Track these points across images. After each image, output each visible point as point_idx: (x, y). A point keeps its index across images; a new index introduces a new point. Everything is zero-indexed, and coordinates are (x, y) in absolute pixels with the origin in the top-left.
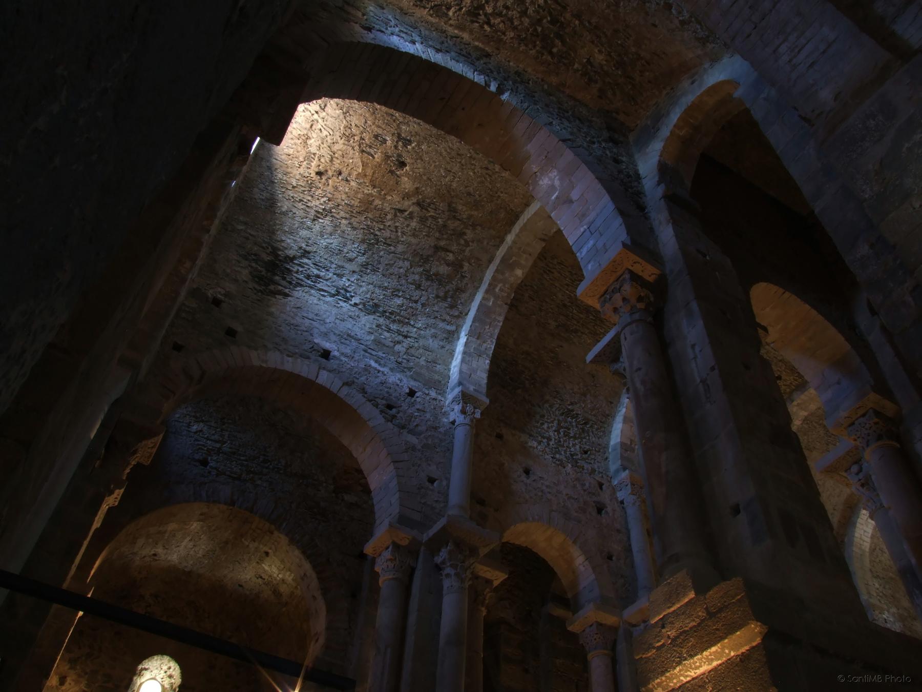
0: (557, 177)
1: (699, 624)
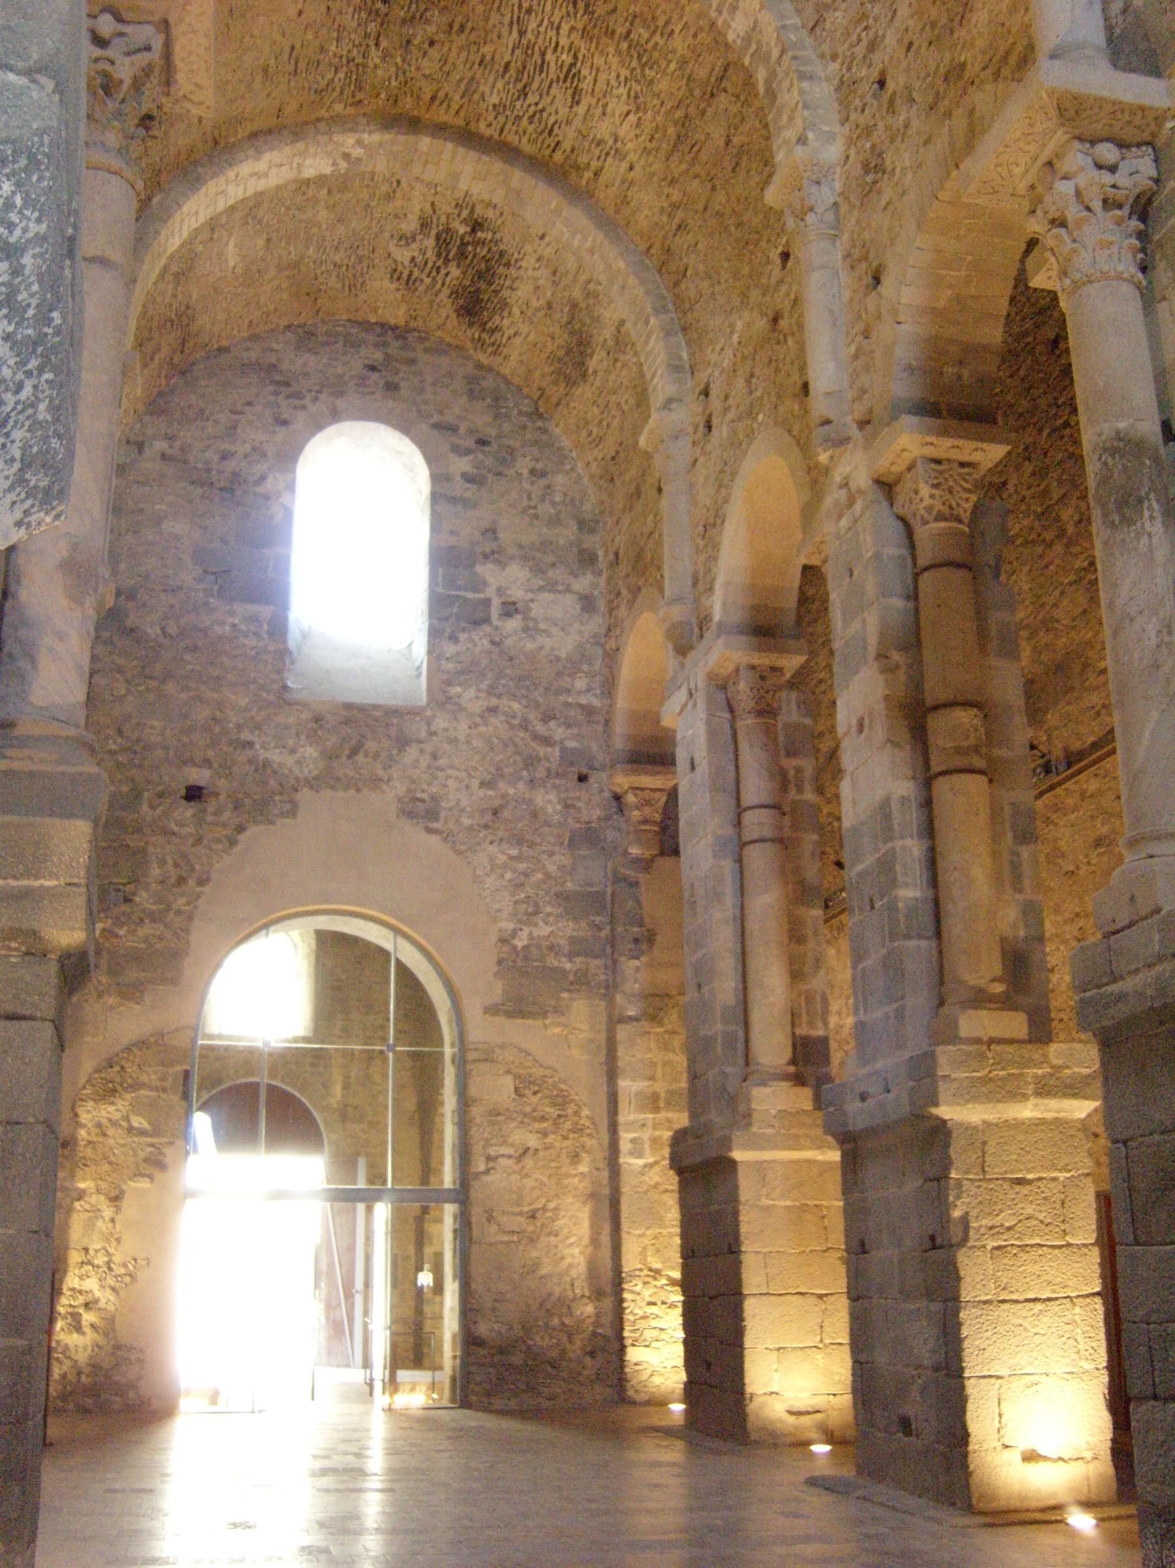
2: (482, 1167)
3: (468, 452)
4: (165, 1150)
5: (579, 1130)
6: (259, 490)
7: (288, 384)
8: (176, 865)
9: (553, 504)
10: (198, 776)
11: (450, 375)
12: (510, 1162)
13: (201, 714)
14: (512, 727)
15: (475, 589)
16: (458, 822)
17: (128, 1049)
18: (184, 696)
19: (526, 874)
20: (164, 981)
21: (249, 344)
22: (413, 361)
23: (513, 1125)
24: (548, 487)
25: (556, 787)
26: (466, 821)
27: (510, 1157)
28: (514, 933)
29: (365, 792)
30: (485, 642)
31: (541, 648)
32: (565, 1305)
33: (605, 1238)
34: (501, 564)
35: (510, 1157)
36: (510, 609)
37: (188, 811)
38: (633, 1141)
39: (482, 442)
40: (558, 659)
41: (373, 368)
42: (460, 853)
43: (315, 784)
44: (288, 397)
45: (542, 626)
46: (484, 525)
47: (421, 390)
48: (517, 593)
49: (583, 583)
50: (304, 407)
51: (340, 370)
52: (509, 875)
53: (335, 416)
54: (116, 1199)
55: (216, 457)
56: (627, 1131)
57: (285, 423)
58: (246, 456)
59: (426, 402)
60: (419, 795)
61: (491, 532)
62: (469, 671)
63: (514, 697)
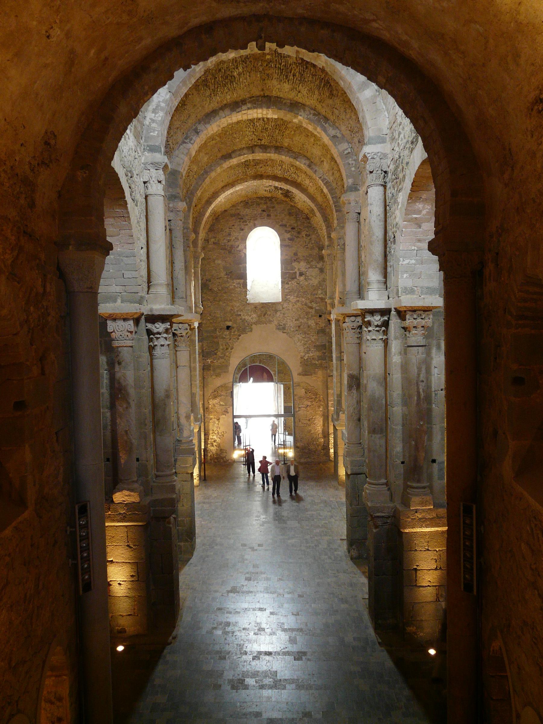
0: (428, 210)
1: (432, 518)
2: (298, 410)
3: (289, 232)
4: (228, 409)
7: (243, 219)
10: (229, 324)
11: (284, 210)
12: (304, 408)
13: (229, 309)
15: (292, 270)
17: (218, 387)
18: (224, 305)
19: (307, 341)
20: (225, 372)
21: (232, 208)
22: (274, 207)
23: (305, 400)
25: (314, 319)
26: (292, 330)
27: (304, 407)
33: (326, 425)
34: (299, 262)
35: (304, 407)
36: (301, 274)
37: (227, 332)
38: (332, 404)
39: (293, 228)
40: (314, 286)
41: (264, 211)
42: (290, 337)
43: (256, 323)
44: (243, 222)
46: (294, 252)
48: (303, 270)
49: (319, 265)
50: (247, 225)
51: (255, 212)
52: (303, 342)
53: (255, 226)
54: (218, 419)
55: (227, 241)
57: (242, 230)
59: (278, 219)
61: (296, 254)
63: (303, 297)
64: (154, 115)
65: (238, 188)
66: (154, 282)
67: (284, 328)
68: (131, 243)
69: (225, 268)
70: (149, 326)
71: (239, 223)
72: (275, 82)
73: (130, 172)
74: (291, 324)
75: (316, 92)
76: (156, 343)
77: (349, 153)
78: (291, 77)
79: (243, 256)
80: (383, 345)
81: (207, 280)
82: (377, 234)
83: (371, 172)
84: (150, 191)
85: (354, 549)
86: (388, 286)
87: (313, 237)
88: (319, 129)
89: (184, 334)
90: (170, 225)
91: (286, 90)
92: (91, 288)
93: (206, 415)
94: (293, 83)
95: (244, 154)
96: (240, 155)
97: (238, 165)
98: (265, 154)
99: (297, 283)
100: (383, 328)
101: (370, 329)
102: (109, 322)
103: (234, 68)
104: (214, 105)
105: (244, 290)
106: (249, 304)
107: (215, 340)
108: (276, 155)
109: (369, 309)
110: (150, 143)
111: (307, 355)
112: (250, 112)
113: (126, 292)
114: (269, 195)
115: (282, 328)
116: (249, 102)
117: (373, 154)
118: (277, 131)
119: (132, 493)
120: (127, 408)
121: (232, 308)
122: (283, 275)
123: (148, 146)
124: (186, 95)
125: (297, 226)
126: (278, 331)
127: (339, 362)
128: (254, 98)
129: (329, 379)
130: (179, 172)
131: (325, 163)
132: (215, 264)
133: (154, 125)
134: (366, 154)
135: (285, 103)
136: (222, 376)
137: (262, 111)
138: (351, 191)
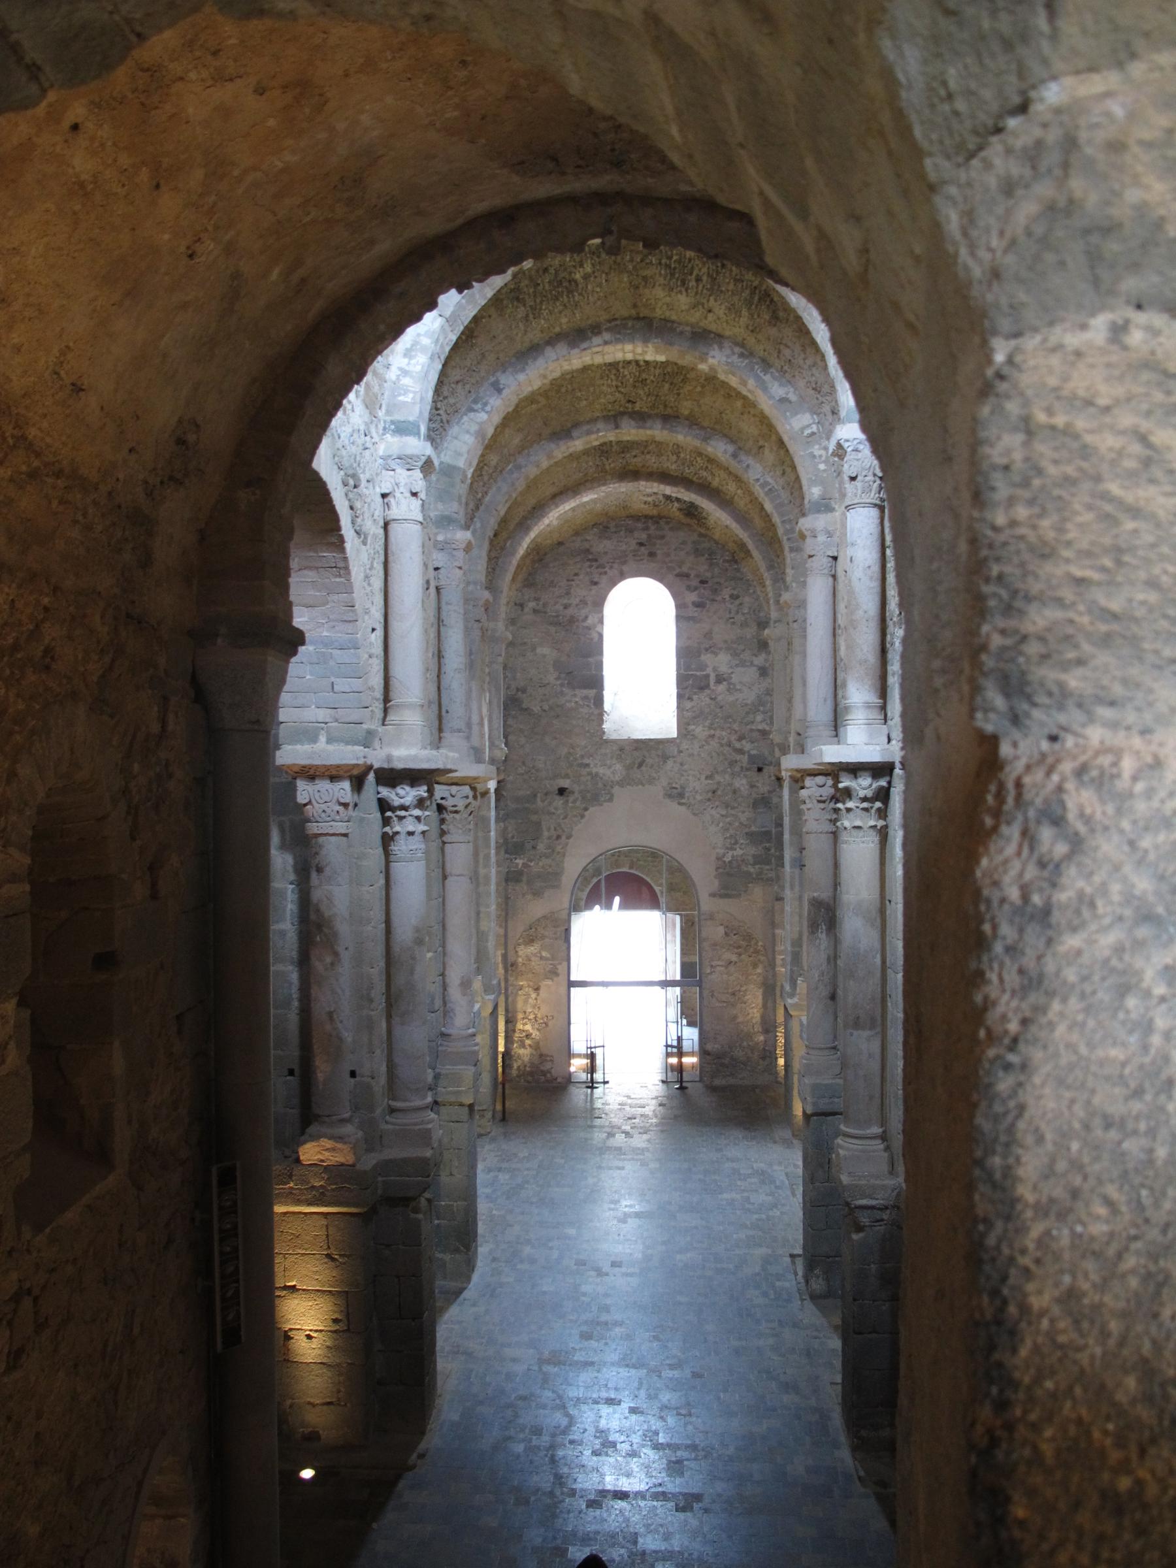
3: (696, 589)
4: (558, 967)
5: (757, 952)
6: (585, 624)
7: (596, 560)
8: (555, 829)
9: (743, 614)
10: (565, 783)
11: (684, 543)
12: (723, 968)
14: (722, 745)
15: (702, 670)
16: (694, 798)
17: (538, 920)
19: (730, 824)
20: (553, 887)
21: (574, 538)
22: (663, 537)
24: (741, 604)
25: (745, 776)
26: (699, 797)
27: (722, 966)
28: (724, 855)
29: (647, 786)
30: (707, 699)
31: (737, 700)
32: (749, 1036)
34: (716, 654)
35: (722, 966)
36: (719, 680)
37: (559, 802)
38: (783, 959)
39: (703, 582)
40: (746, 705)
41: (641, 544)
42: (695, 814)
43: (621, 784)
44: (597, 568)
45: (738, 687)
47: (668, 555)
48: (724, 669)
49: (760, 660)
50: (606, 573)
51: (624, 547)
52: (721, 825)
53: (622, 576)
54: (537, 989)
55: (561, 608)
56: (779, 954)
57: (596, 583)
58: (577, 605)
59: (671, 562)
60: (674, 785)
61: (708, 635)
62: (699, 716)
63: (723, 729)
64: (406, 360)
65: (587, 497)
66: (397, 698)
67: (681, 795)
68: (350, 621)
69: (557, 665)
70: (385, 792)
71: (588, 570)
72: (659, 292)
73: (354, 476)
74: (696, 785)
75: (745, 312)
76: (397, 828)
77: (813, 434)
78: (693, 283)
79: (596, 639)
80: (877, 839)
81: (518, 690)
82: (865, 607)
83: (853, 479)
84: (395, 512)
85: (818, 1277)
86: (889, 714)
87: (747, 600)
88: (751, 383)
89: (461, 807)
90: (437, 579)
91: (684, 308)
92: (258, 722)
93: (511, 979)
94: (697, 293)
95: (599, 431)
96: (589, 433)
97: (586, 452)
98: (641, 431)
99: (711, 699)
100: (878, 804)
101: (850, 804)
102: (301, 785)
103: (575, 267)
104: (535, 335)
105: (596, 712)
106: (607, 741)
107: (534, 818)
108: (665, 432)
109: (848, 763)
110: (397, 417)
111: (731, 853)
112: (609, 348)
113: (336, 721)
114: (655, 512)
115: (677, 794)
116: (607, 330)
117: (855, 442)
118: (667, 386)
119: (339, 1146)
120: (332, 964)
121: (571, 750)
122: (682, 680)
123: (392, 422)
124: (476, 319)
125: (712, 577)
126: (668, 801)
127: (797, 871)
128: (618, 322)
129: (777, 905)
130: (459, 468)
131: (767, 451)
132: (536, 655)
133: (406, 381)
134: (842, 442)
135: (682, 333)
136: (546, 894)
137: (634, 348)
138: (819, 511)
